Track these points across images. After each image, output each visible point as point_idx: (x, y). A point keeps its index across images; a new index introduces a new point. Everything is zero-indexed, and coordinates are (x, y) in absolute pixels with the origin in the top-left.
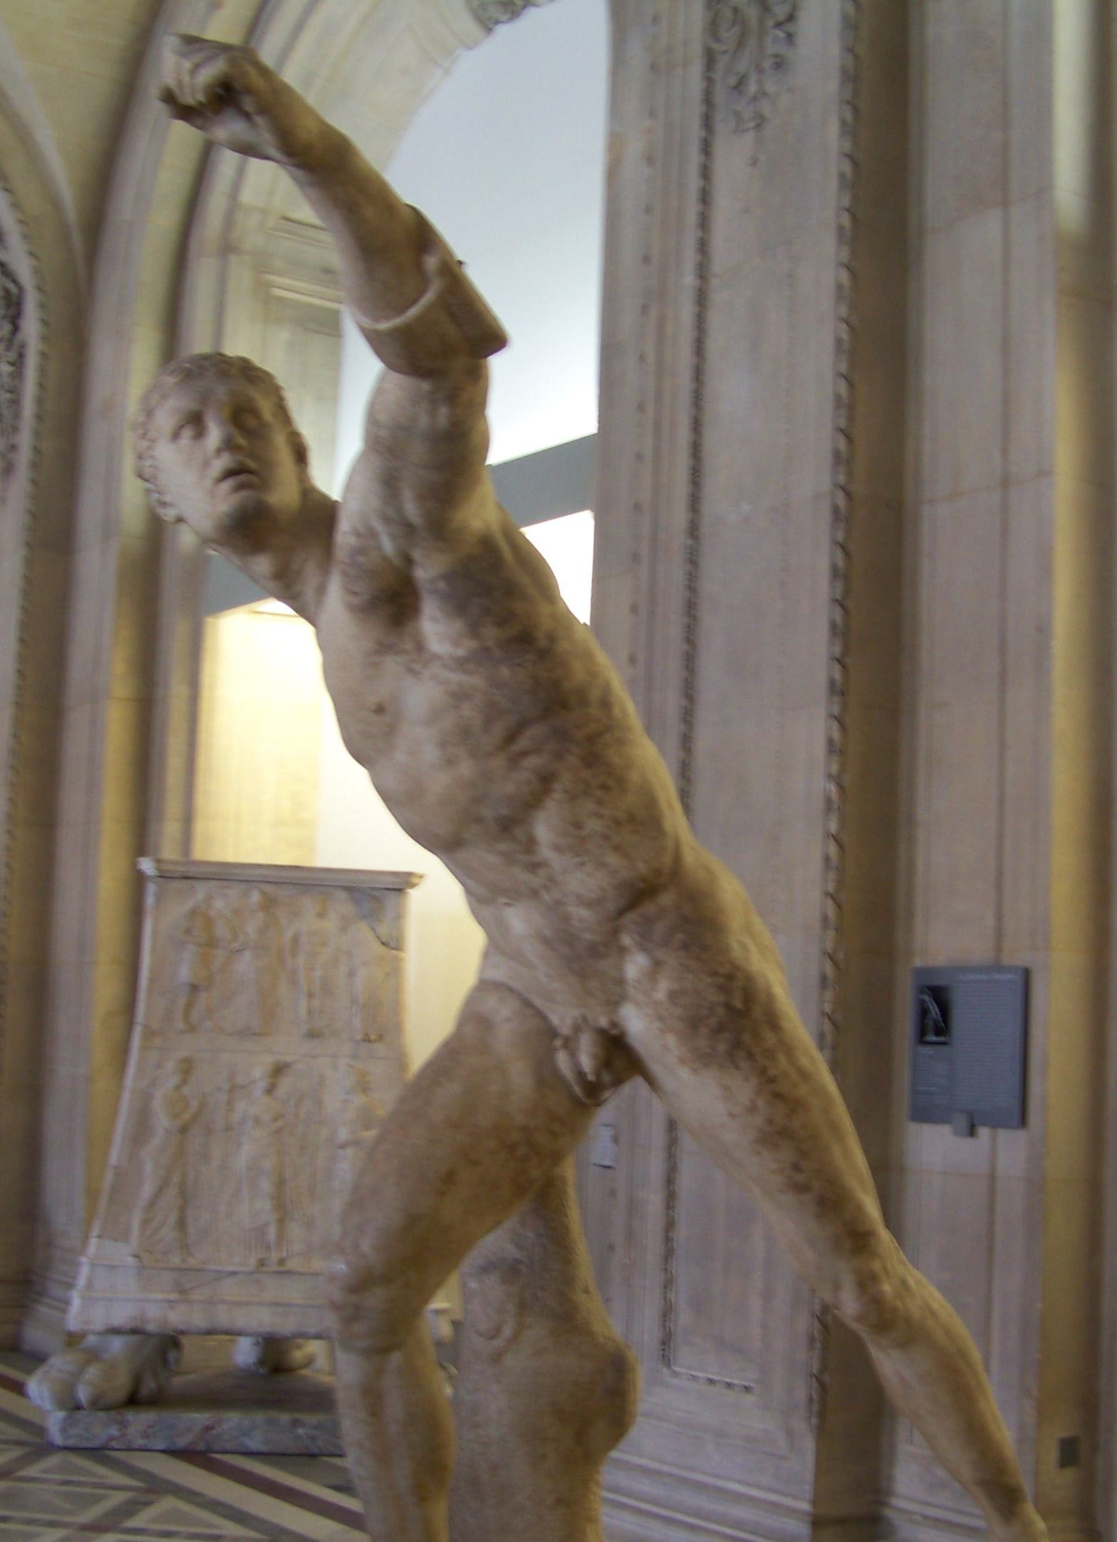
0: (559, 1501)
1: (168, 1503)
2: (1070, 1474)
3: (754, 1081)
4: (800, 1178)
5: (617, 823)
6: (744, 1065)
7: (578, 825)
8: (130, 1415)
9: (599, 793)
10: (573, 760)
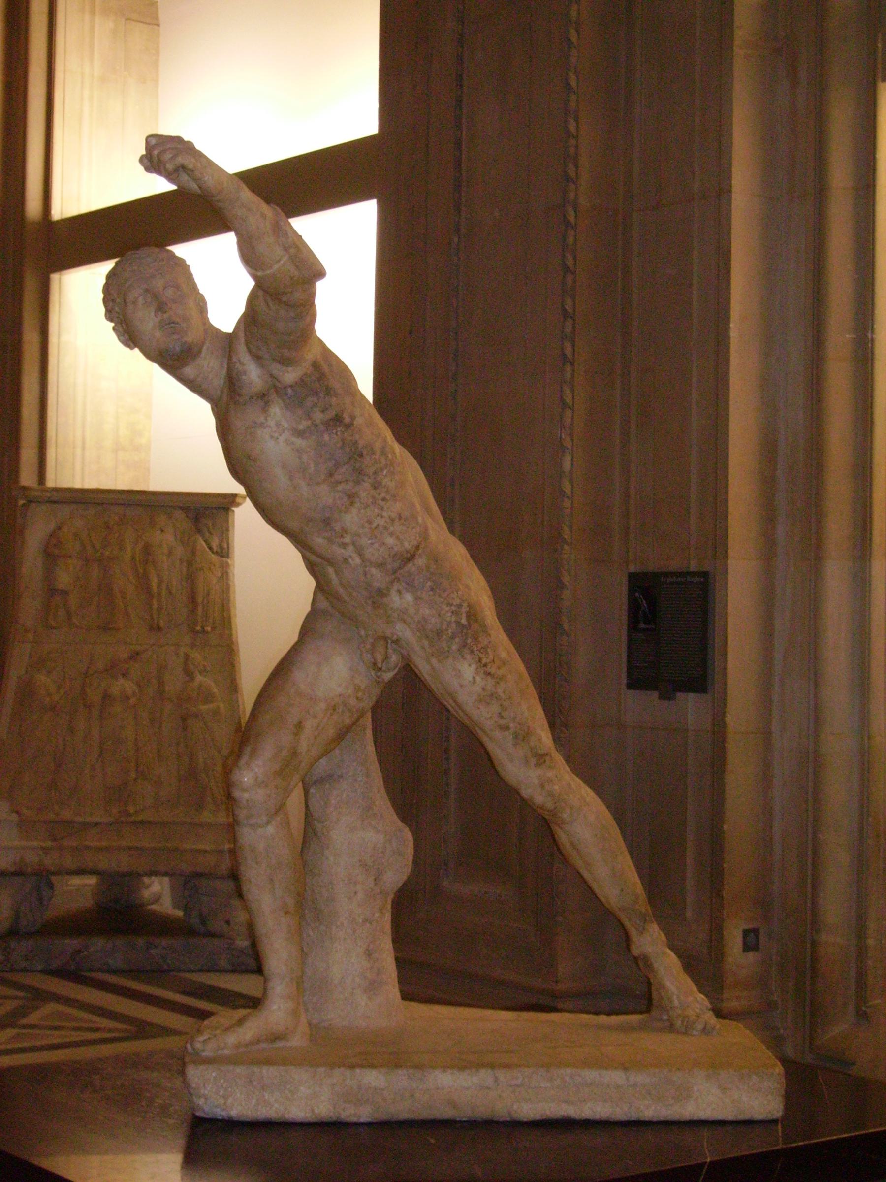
0: (365, 920)
1: (51, 1007)
2: (751, 955)
3: (474, 666)
4: (502, 722)
5: (393, 520)
6: (468, 656)
7: (370, 522)
8: (13, 944)
9: (381, 503)
10: (367, 485)
